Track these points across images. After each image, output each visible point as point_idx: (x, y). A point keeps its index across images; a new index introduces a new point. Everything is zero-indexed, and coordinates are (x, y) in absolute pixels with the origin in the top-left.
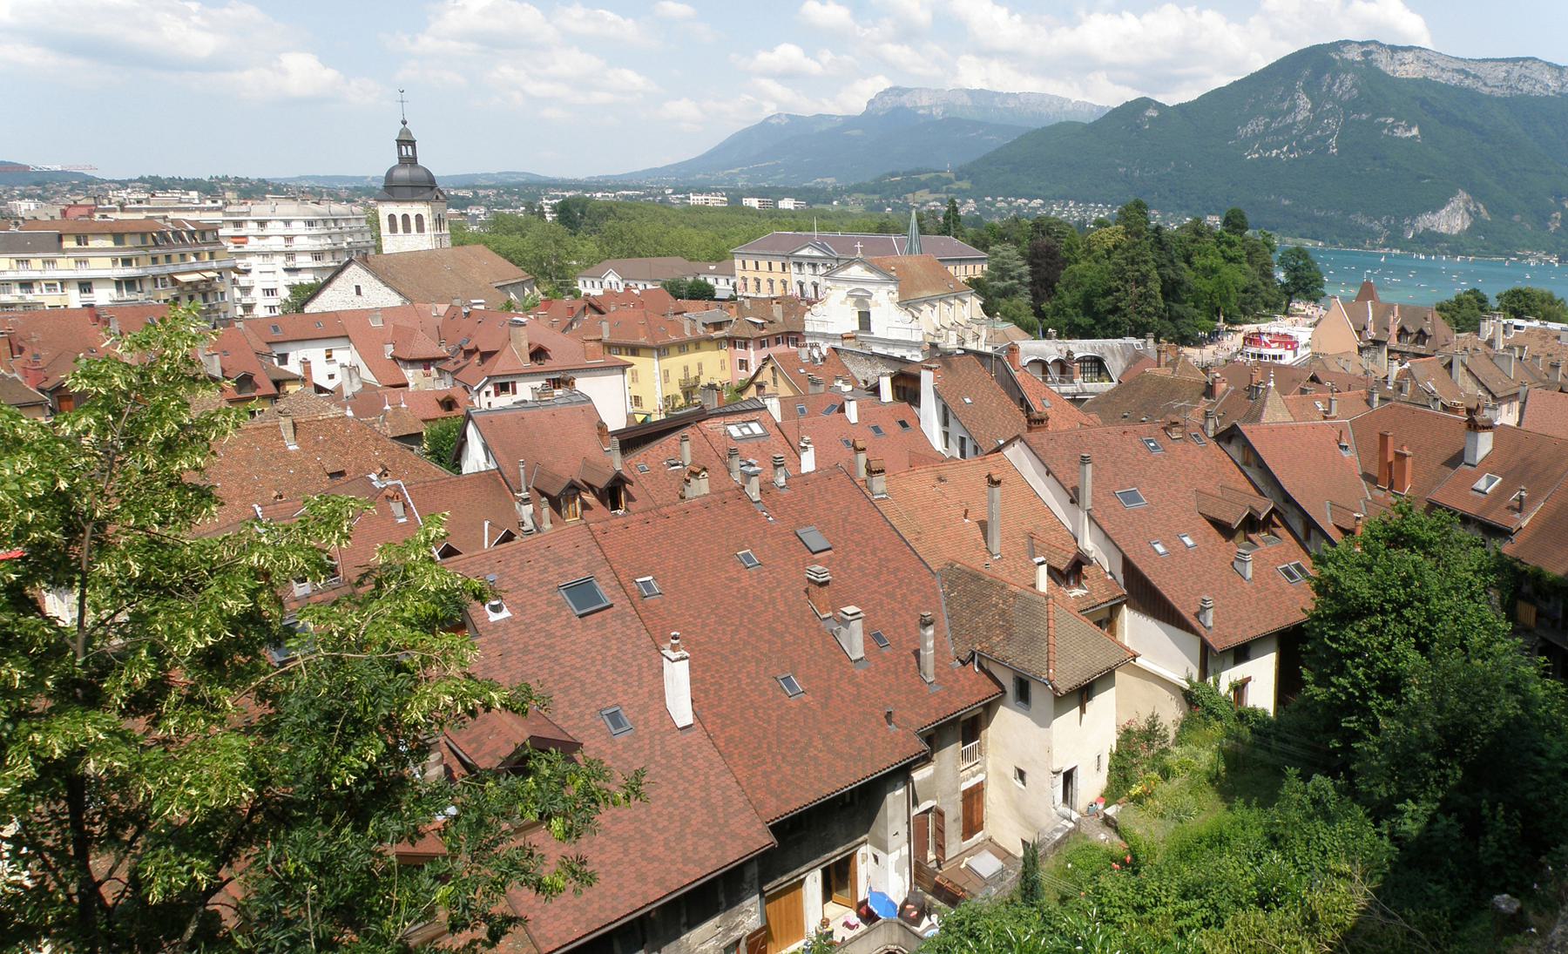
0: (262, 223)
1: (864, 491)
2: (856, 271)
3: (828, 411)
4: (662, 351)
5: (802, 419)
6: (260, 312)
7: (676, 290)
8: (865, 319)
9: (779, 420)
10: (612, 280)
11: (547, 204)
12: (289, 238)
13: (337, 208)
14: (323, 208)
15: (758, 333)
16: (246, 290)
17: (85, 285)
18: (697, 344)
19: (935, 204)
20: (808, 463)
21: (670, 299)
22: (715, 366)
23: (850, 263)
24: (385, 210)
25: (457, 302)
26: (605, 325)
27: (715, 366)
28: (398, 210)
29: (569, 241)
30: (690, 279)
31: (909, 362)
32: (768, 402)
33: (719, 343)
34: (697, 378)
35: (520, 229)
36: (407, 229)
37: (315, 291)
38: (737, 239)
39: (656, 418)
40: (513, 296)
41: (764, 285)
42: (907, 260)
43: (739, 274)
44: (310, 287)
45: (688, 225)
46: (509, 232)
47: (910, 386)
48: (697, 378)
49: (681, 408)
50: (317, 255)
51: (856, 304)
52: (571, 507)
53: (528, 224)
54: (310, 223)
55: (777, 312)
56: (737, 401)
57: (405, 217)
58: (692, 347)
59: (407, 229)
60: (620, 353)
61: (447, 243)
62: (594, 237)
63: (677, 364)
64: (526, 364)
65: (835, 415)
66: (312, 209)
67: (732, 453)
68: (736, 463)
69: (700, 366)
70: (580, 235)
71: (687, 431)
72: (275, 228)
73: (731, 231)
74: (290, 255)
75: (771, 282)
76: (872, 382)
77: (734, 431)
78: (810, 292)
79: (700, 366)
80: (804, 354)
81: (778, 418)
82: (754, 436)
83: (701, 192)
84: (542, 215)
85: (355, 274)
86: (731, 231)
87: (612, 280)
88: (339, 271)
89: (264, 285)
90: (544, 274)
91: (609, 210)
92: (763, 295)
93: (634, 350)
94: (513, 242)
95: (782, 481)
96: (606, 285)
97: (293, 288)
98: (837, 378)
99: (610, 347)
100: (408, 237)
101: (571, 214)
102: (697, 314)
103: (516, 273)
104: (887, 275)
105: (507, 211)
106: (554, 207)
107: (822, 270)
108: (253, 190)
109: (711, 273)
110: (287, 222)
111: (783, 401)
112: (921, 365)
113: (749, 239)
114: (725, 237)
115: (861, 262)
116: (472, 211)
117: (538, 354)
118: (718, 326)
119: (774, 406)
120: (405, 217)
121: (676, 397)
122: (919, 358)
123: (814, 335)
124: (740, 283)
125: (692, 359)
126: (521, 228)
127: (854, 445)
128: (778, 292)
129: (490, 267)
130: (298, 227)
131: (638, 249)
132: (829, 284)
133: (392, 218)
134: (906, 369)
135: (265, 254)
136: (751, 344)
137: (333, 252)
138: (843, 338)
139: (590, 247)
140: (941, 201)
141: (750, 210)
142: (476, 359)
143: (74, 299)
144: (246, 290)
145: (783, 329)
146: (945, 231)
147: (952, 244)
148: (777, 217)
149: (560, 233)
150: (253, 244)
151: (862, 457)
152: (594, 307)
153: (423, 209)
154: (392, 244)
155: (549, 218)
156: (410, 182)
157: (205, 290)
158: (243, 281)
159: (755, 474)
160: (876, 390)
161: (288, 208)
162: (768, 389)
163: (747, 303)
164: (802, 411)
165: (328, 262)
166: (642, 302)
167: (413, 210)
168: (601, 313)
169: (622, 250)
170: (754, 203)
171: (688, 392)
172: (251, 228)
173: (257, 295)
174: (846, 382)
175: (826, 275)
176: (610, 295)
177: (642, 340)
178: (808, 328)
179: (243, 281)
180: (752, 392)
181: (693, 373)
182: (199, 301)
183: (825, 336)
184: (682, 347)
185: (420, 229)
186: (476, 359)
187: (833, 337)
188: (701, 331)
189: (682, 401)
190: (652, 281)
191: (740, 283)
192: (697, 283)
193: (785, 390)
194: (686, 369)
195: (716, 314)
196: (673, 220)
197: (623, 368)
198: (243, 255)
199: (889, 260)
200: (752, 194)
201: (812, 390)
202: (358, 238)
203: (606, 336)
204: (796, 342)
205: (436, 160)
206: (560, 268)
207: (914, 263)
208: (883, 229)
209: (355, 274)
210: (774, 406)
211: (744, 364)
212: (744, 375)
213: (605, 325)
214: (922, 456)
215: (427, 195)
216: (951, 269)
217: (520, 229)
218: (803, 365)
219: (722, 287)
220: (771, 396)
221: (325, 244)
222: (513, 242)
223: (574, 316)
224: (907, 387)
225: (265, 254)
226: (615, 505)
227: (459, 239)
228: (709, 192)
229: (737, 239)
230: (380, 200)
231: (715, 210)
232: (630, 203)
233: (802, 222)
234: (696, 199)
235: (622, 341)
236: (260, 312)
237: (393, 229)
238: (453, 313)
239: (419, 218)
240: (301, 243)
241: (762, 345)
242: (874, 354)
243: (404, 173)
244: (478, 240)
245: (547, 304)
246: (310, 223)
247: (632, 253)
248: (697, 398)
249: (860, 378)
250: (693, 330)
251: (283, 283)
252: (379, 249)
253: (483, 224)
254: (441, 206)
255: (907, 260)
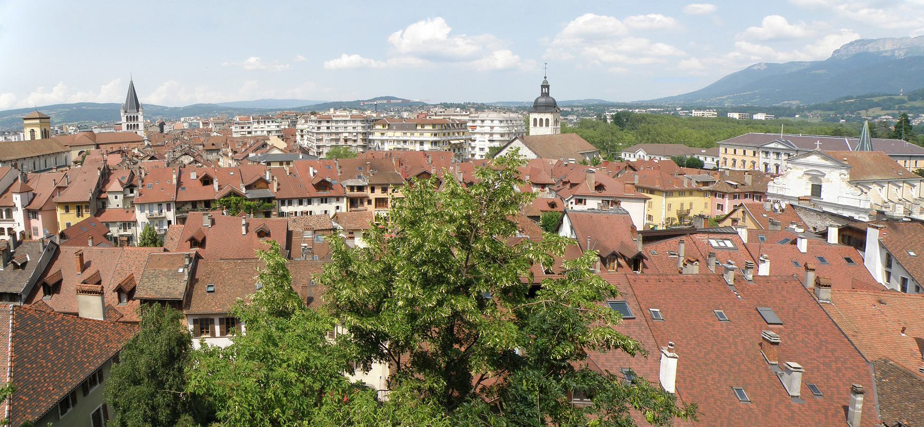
0: (482, 121)
1: (813, 296)
2: (814, 159)
3: (783, 242)
4: (669, 193)
5: (762, 243)
6: (477, 157)
7: (680, 162)
8: (817, 190)
9: (745, 241)
10: (641, 153)
11: (608, 115)
12: (492, 128)
13: (512, 115)
14: (507, 115)
15: (732, 190)
16: (473, 148)
17: (422, 143)
18: (691, 192)
19: (889, 118)
20: (764, 269)
21: (677, 166)
22: (700, 205)
23: (809, 154)
24: (533, 116)
25: (562, 159)
26: (637, 177)
27: (700, 205)
28: (538, 116)
29: (619, 134)
30: (689, 157)
31: (856, 221)
32: (739, 230)
33: (705, 193)
34: (688, 211)
35: (593, 127)
36: (541, 125)
37: (500, 150)
38: (722, 136)
39: (660, 228)
40: (588, 158)
41: (739, 163)
42: (859, 155)
43: (722, 155)
44: (498, 148)
45: (689, 127)
46: (588, 128)
47: (859, 237)
48: (688, 211)
49: (676, 225)
50: (502, 135)
51: (810, 179)
52: (612, 264)
53: (598, 124)
54: (501, 121)
55: (748, 179)
56: (713, 226)
57: (541, 120)
58: (687, 193)
59: (541, 125)
60: (643, 192)
61: (559, 132)
62: (633, 132)
63: (677, 202)
64: (592, 191)
65: (788, 246)
66: (502, 116)
67: (711, 255)
68: (713, 261)
69: (691, 204)
70: (625, 131)
71: (683, 238)
72: (488, 123)
73: (720, 130)
74: (491, 134)
75: (744, 162)
76: (820, 229)
77: (714, 243)
78: (773, 170)
79: (691, 204)
80: (767, 206)
81: (745, 240)
82: (727, 248)
83: (699, 109)
84: (605, 120)
85: (517, 143)
86: (720, 130)
87: (641, 153)
88: (510, 142)
89: (480, 146)
90: (604, 149)
91: (642, 118)
92: (737, 169)
93: (652, 191)
94: (590, 132)
95: (750, 277)
96: (637, 156)
97: (490, 148)
98: (792, 223)
99: (638, 188)
100: (541, 129)
101: (626, 120)
102: (691, 177)
103: (590, 148)
104: (840, 163)
105: (588, 118)
106: (612, 116)
107: (784, 157)
108: (480, 108)
109: (703, 154)
110: (492, 121)
111: (750, 231)
112: (868, 224)
113: (730, 136)
114: (714, 134)
115: (818, 153)
116: (570, 117)
117: (599, 187)
118: (706, 183)
119: (743, 234)
120: (541, 120)
121: (674, 219)
122: (867, 219)
123: (773, 195)
124: (721, 161)
125: (686, 200)
126: (593, 126)
127: (806, 266)
128: (748, 167)
129: (578, 144)
130: (496, 123)
131: (658, 139)
132: (790, 165)
133: (535, 120)
134: (853, 225)
135: (482, 134)
136: (727, 196)
137: (509, 134)
138: (799, 199)
139: (630, 136)
140: (894, 116)
141: (733, 120)
142: (568, 186)
143: (418, 148)
144: (473, 148)
145: (754, 190)
146: (897, 135)
147: (904, 145)
148: (752, 124)
149: (615, 129)
150: (478, 130)
151: (811, 276)
152: (631, 167)
153: (549, 116)
154: (534, 131)
155: (609, 121)
156: (546, 104)
157: (459, 147)
158: (473, 144)
159: (732, 270)
160: (824, 235)
161: (493, 115)
162: (740, 223)
163: (727, 173)
164: (762, 239)
165: (506, 138)
166: (659, 167)
167: (544, 116)
168: (635, 170)
169: (648, 139)
170: (736, 116)
171: (682, 216)
172: (478, 123)
173: (477, 151)
174: (798, 226)
175: (788, 160)
176: (641, 161)
177: (657, 186)
178: (770, 191)
179: (473, 144)
180: (728, 222)
181: (686, 207)
182: (457, 151)
183: (783, 197)
184: (682, 193)
185: (547, 125)
186: (568, 186)
187: (790, 198)
188: (694, 185)
189: (677, 221)
190: (664, 156)
191: (721, 161)
192: (693, 159)
193: (752, 226)
194: (682, 205)
195: (705, 177)
196: (680, 124)
197: (645, 200)
198: (474, 134)
199: (842, 153)
200: (734, 110)
201: (771, 227)
202: (520, 128)
203: (636, 182)
204: (760, 198)
205: (557, 94)
206: (613, 147)
207: (866, 157)
208: (838, 133)
209: (517, 143)
210: (743, 234)
211: (720, 207)
212: (719, 212)
213: (637, 177)
214: (865, 283)
215: (552, 110)
216: (901, 162)
217: (593, 127)
218: (766, 212)
219: (709, 162)
220: (742, 227)
221: (505, 130)
222: (590, 132)
223: (620, 170)
224: (853, 236)
225: (482, 134)
226: (636, 268)
227: (564, 131)
228: (705, 109)
229: (722, 136)
230: (530, 112)
231: (708, 119)
232: (655, 115)
233: (771, 128)
234: (695, 113)
235: (645, 186)
236: (477, 157)
237: (535, 125)
238: (559, 164)
239: (547, 120)
240: (496, 130)
241: (735, 197)
242: (824, 212)
243: (543, 100)
244: (573, 131)
245: (606, 163)
246: (501, 121)
247: (654, 141)
248: (687, 221)
249: (811, 226)
250: (689, 184)
251: (487, 145)
252: (528, 133)
253: (575, 124)
254: (557, 115)
255: (859, 155)
